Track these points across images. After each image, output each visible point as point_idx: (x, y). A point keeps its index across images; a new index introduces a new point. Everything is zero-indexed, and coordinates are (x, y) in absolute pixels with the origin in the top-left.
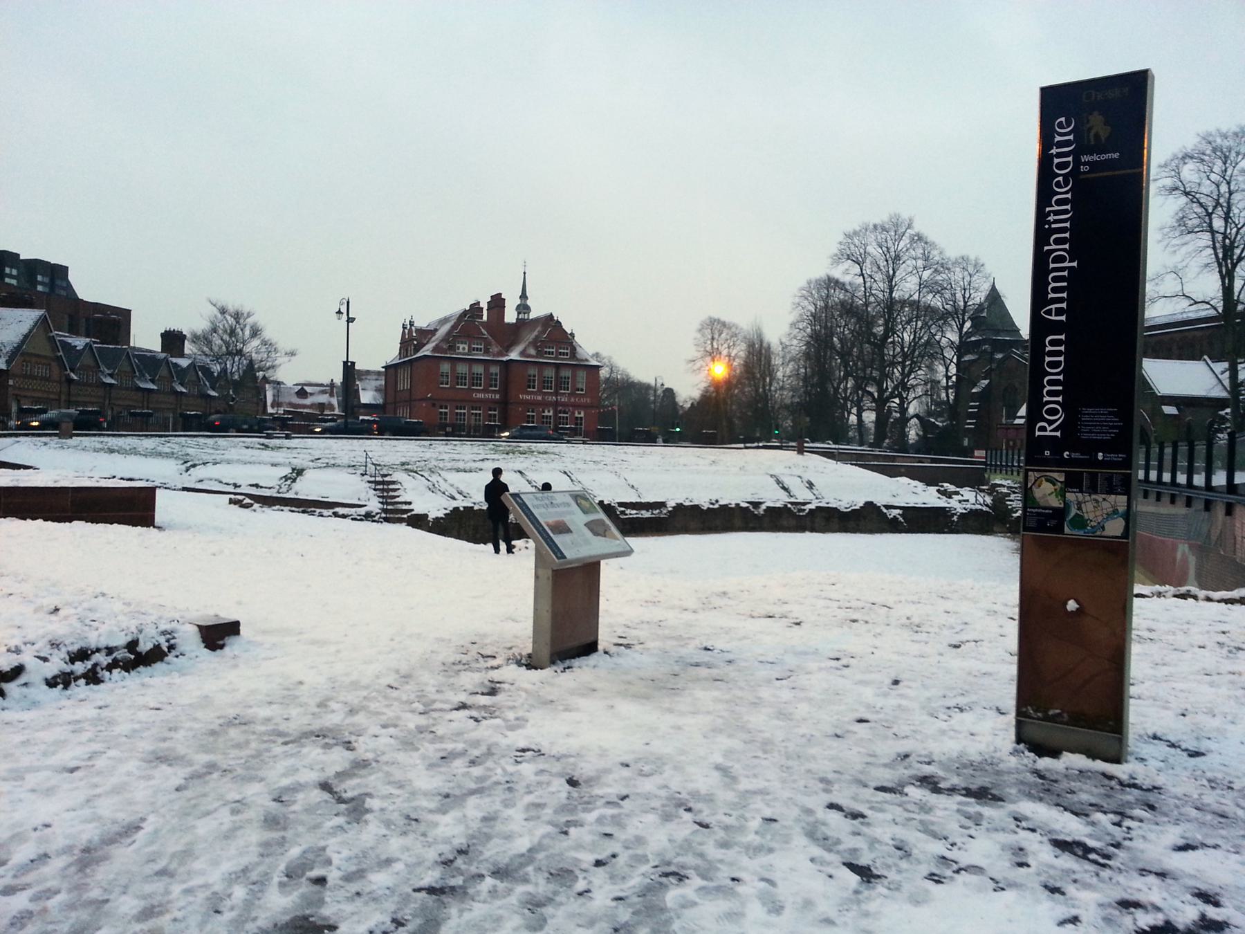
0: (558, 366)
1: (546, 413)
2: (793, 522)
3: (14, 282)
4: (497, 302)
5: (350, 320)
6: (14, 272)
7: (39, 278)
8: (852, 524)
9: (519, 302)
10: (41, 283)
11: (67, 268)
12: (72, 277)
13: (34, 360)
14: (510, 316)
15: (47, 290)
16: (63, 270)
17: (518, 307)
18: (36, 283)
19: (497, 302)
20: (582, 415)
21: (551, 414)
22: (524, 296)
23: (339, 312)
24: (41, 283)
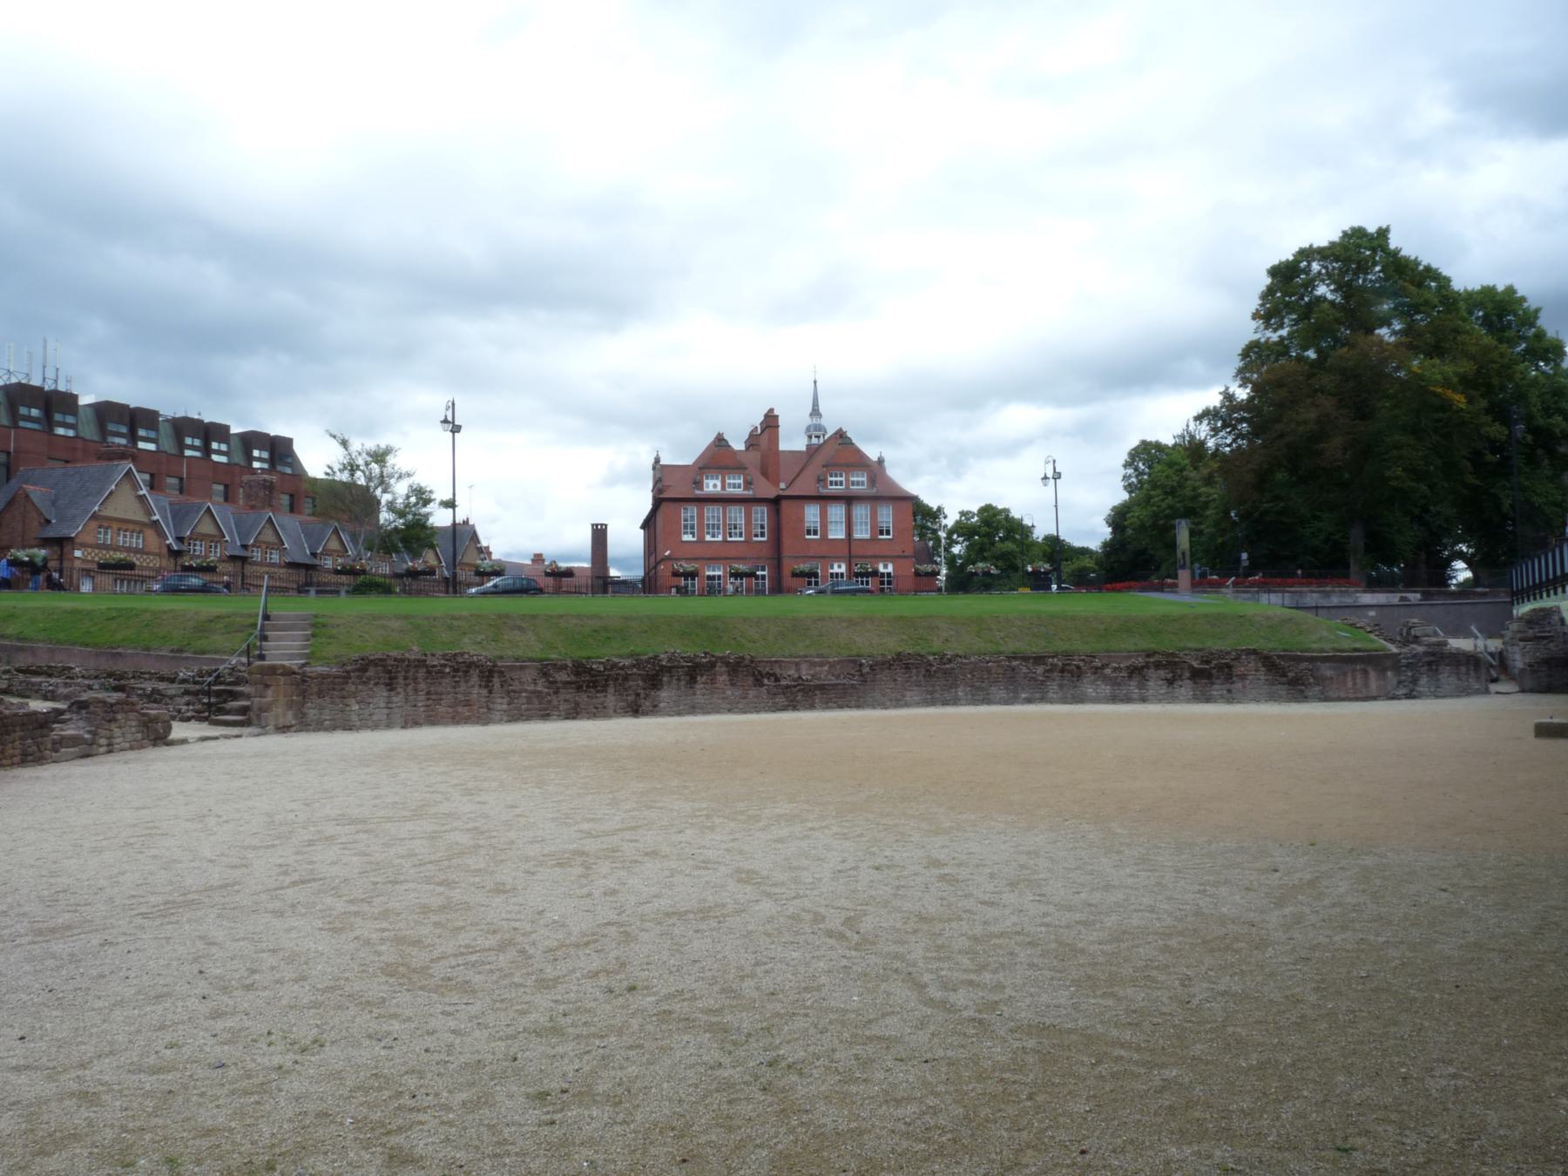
0: (849, 500)
1: (836, 570)
2: (1106, 690)
3: (223, 459)
4: (771, 422)
5: (456, 429)
6: (224, 447)
7: (256, 453)
8: (1218, 689)
9: (808, 421)
10: (259, 459)
11: (289, 441)
12: (299, 449)
13: (115, 526)
14: (792, 441)
15: (266, 466)
16: (289, 441)
17: (808, 429)
18: (250, 459)
19: (771, 422)
20: (890, 569)
21: (843, 569)
22: (815, 412)
23: (445, 421)
24: (259, 459)
